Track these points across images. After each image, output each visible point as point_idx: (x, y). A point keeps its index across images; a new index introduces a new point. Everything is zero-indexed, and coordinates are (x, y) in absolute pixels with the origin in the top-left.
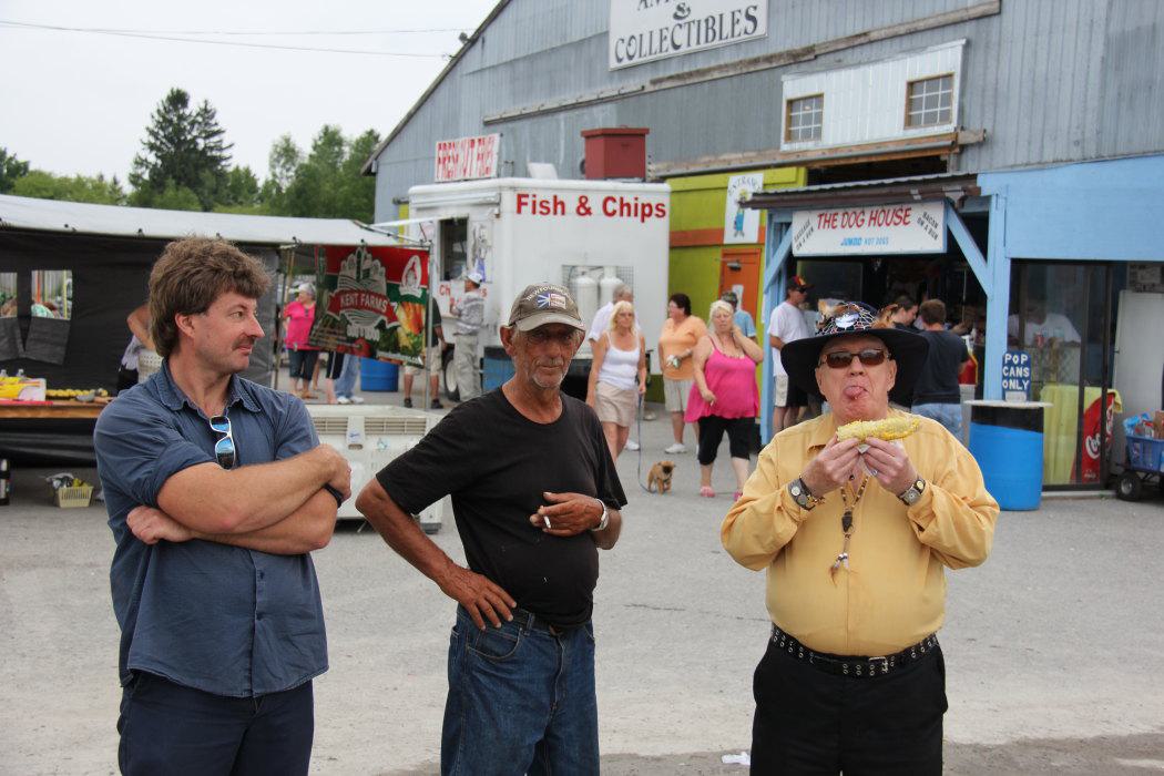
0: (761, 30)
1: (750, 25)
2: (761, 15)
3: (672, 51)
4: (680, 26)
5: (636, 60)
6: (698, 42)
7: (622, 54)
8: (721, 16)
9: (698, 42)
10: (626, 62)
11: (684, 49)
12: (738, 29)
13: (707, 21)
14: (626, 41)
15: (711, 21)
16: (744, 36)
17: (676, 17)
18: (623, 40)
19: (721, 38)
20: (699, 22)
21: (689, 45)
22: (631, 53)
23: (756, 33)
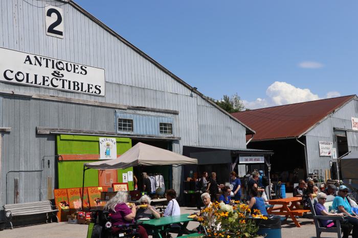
0: (102, 94)
1: (98, 92)
2: (102, 89)
3: (51, 86)
4: (57, 80)
5: (24, 82)
6: (69, 88)
7: (9, 75)
8: (82, 84)
9: (69, 88)
10: (14, 81)
11: (60, 87)
12: (91, 91)
13: (74, 82)
14: (15, 72)
15: (76, 84)
16: (94, 93)
17: (53, 74)
18: (12, 72)
19: (82, 90)
20: (69, 82)
21: (63, 87)
22: (20, 77)
23: (100, 94)
